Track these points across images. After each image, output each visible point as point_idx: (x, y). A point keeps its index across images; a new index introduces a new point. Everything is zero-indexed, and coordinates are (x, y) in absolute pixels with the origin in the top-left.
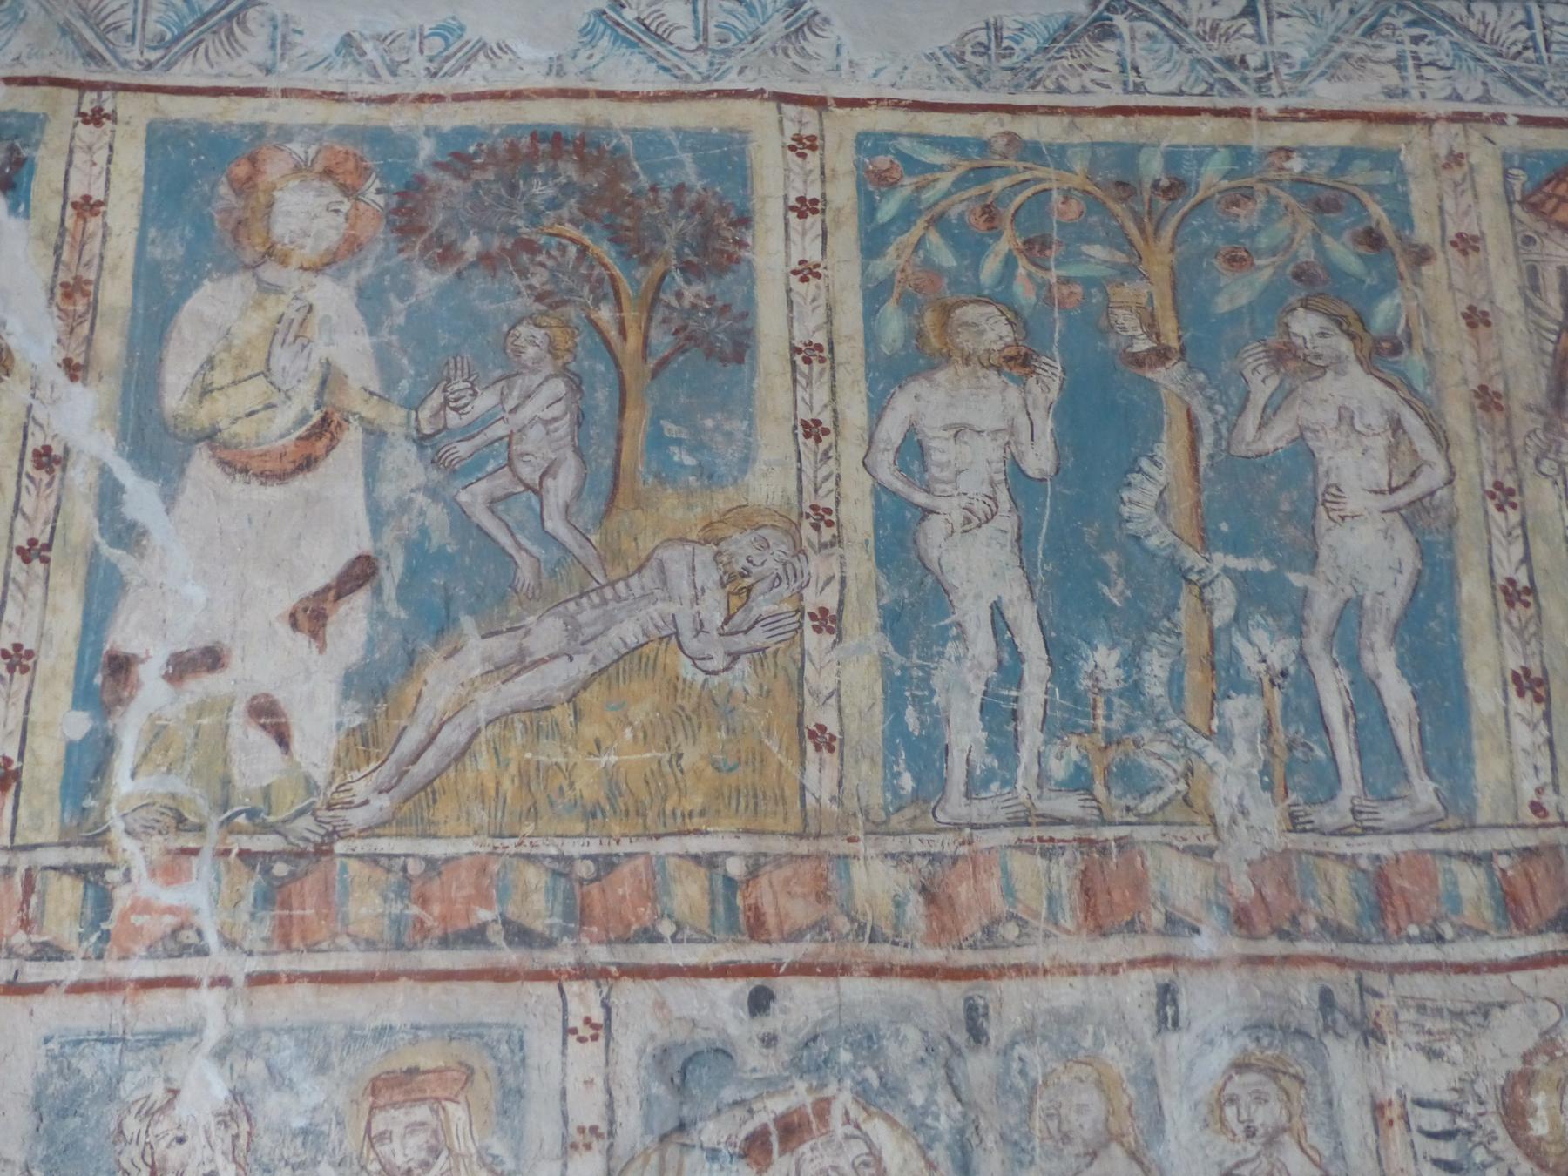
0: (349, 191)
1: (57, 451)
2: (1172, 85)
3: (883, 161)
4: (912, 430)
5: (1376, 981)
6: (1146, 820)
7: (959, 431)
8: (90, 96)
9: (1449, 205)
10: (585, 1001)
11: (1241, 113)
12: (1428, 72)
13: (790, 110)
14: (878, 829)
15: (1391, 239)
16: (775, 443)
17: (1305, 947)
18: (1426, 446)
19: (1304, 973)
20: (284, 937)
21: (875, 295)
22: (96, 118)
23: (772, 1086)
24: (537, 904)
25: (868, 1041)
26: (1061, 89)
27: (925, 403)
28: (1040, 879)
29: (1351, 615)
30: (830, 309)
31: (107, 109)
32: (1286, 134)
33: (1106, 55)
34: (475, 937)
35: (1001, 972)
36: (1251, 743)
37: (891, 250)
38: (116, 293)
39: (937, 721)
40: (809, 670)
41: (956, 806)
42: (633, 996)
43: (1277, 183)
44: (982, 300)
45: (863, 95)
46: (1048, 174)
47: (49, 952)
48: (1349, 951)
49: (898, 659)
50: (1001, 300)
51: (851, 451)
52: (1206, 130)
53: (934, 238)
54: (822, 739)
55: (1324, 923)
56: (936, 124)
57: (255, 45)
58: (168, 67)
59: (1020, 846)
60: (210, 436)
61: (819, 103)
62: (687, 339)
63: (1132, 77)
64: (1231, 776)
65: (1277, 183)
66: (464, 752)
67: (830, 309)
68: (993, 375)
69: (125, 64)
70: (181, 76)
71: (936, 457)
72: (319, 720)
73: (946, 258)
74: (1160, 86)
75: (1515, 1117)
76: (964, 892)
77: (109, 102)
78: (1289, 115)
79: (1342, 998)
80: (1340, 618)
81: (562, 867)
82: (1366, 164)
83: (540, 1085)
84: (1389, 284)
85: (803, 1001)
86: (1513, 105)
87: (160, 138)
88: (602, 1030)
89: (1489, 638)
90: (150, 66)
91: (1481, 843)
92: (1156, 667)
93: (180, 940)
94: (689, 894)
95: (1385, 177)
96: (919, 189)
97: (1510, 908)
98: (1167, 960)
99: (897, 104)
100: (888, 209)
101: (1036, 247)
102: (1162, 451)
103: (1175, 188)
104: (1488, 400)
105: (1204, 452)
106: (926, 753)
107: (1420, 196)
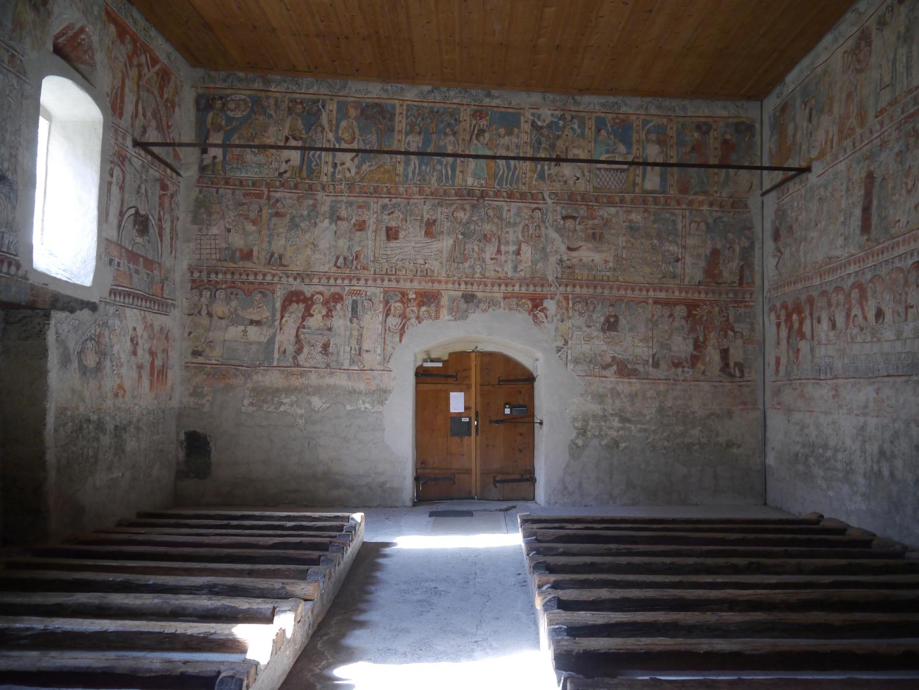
10: (375, 200)
16: (396, 142)
24: (372, 189)
27: (410, 138)
28: (416, 189)
29: (447, 164)
38: (334, 122)
52: (442, 105)
57: (347, 91)
64: (434, 180)
70: (340, 94)
72: (353, 171)
74: (438, 99)
75: (453, 214)
85: (394, 201)
86: (473, 103)
87: (338, 103)
93: (342, 192)
94: (385, 190)
97: (456, 194)
101: (423, 119)
103: (437, 112)
104: (464, 140)
106: (406, 176)
107: (462, 114)
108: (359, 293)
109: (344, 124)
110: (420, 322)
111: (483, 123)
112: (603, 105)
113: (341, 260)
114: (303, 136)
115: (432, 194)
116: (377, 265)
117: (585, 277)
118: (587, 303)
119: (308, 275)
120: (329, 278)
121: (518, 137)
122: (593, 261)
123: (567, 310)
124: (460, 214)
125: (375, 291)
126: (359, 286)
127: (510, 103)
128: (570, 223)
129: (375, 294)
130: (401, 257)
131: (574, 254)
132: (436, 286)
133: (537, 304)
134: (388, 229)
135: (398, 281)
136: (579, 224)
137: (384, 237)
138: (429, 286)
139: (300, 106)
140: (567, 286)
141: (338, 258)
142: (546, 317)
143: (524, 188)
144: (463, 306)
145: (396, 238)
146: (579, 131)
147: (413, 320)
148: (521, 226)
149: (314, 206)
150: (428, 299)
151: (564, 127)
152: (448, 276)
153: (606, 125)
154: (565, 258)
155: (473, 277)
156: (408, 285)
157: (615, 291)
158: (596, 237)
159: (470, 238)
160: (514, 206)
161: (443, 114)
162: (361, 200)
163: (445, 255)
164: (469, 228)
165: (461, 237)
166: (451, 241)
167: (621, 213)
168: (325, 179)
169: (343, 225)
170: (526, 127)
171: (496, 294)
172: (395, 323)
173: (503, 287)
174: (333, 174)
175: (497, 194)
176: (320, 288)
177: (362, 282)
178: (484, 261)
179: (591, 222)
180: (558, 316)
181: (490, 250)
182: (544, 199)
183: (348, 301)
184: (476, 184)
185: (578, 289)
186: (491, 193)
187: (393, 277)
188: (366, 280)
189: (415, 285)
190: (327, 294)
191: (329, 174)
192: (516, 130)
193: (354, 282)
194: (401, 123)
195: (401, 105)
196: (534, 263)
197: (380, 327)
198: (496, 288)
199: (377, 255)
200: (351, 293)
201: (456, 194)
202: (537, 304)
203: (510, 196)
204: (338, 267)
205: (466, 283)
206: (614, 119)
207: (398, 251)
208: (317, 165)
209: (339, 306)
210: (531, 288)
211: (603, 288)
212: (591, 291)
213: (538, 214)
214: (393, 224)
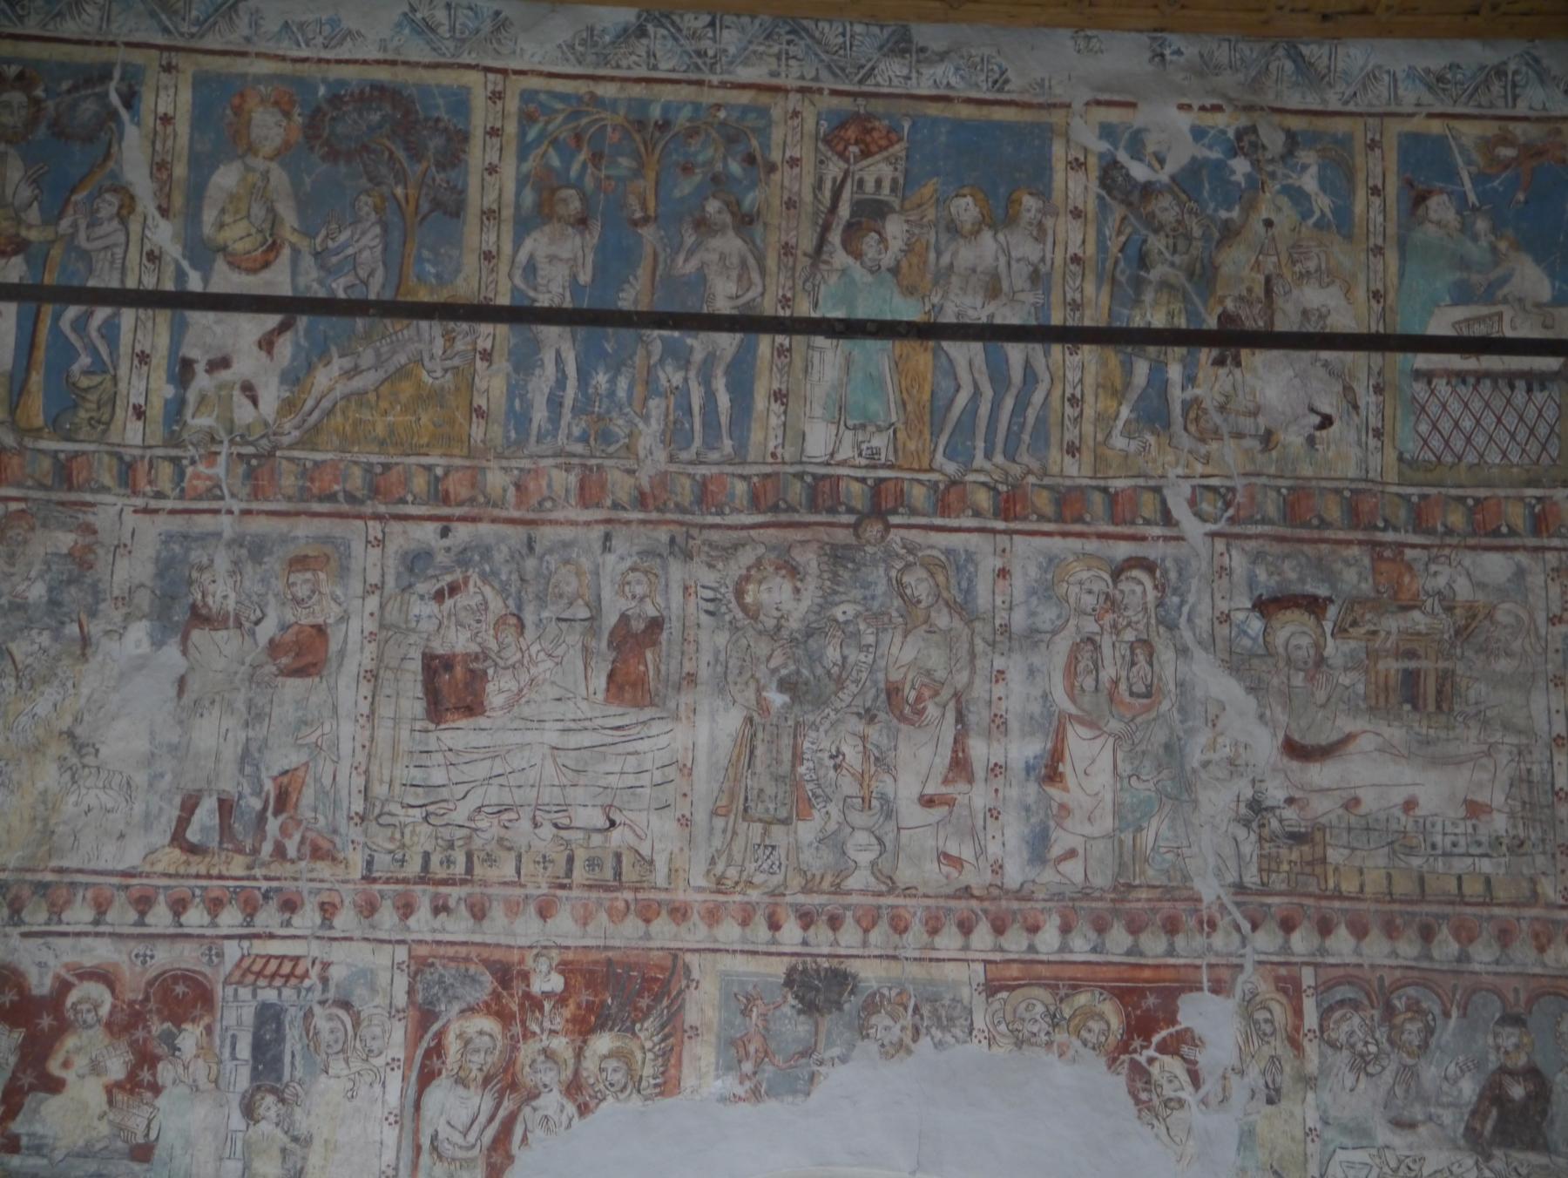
0: (287, 114)
1: (157, 253)
2: (669, 66)
3: (532, 107)
4: (531, 257)
5: (694, 532)
6: (610, 456)
7: (552, 259)
8: (165, 55)
9: (789, 140)
10: (375, 528)
11: (700, 83)
12: (792, 62)
13: (491, 76)
14: (500, 456)
15: (759, 158)
16: (471, 262)
17: (669, 516)
18: (755, 276)
19: (664, 528)
20: (255, 494)
21: (522, 182)
22: (168, 68)
23: (448, 570)
24: (357, 479)
25: (486, 553)
26: (618, 66)
27: (537, 244)
30: (501, 190)
31: (174, 62)
32: (720, 95)
33: (641, 47)
34: (332, 497)
35: (544, 522)
36: (658, 421)
37: (531, 158)
38: (180, 171)
39: (528, 406)
40: (477, 379)
41: (532, 447)
42: (396, 527)
43: (711, 125)
44: (569, 186)
45: (525, 67)
46: (606, 115)
47: (159, 495)
48: (688, 518)
49: (514, 376)
50: (578, 185)
51: (504, 268)
52: (686, 92)
53: (551, 151)
54: (481, 413)
55: (677, 505)
56: (559, 86)
57: (243, 26)
58: (202, 37)
59: (556, 466)
60: (223, 249)
61: (504, 72)
62: (437, 204)
63: (652, 60)
64: (649, 435)
65: (711, 125)
66: (330, 412)
67: (501, 190)
68: (570, 230)
69: (182, 35)
70: (211, 42)
71: (540, 273)
73: (556, 162)
74: (665, 66)
75: (740, 593)
76: (532, 486)
77: (176, 59)
78: (723, 85)
79: (680, 539)
80: (705, 361)
81: (368, 468)
82: (754, 115)
83: (356, 565)
84: (754, 185)
85: (462, 532)
86: (829, 83)
88: (381, 543)
89: (767, 373)
90: (192, 36)
91: (747, 470)
92: (623, 383)
94: (420, 483)
95: (762, 123)
96: (547, 123)
97: (755, 502)
98: (608, 521)
99: (540, 74)
100: (532, 134)
101: (597, 157)
102: (640, 272)
103: (664, 126)
104: (787, 249)
105: (658, 273)
106: (521, 420)
107: (777, 134)
108: (288, 972)
109: (226, 178)
110: (583, 1110)
111: (878, 172)
112: (1437, 82)
113: (206, 814)
114: (33, 235)
115: (641, 501)
116: (382, 839)
117: (1375, 881)
118: (1389, 1011)
119: (42, 888)
120: (143, 903)
121: (1040, 234)
122: (1409, 805)
123: (1296, 1045)
124: (775, 594)
125: (369, 962)
126: (299, 937)
127: (1000, 83)
128: (1292, 630)
129: (367, 976)
130: (494, 795)
131: (1319, 774)
132: (663, 933)
133: (1145, 1015)
134: (435, 667)
135: (479, 913)
136: (1340, 631)
137: (413, 703)
138: (627, 934)
139: (17, 97)
140: (1288, 926)
141: (189, 806)
142: (1195, 1079)
143: (1071, 466)
144: (793, 1027)
145: (473, 707)
146: (1323, 203)
147: (551, 1101)
148: (1063, 645)
149: (81, 560)
150: (624, 993)
151: (1255, 185)
152: (720, 885)
153: (1451, 174)
154: (1276, 793)
155: (837, 890)
156: (529, 929)
157: (1524, 954)
158: (1420, 693)
159: (821, 702)
160: (1027, 553)
161: (692, 132)
162: (304, 529)
163: (704, 785)
164: (814, 659)
165: (777, 699)
166: (732, 721)
167: (1536, 580)
168: (133, 433)
169: (219, 650)
170: (1079, 188)
171: (951, 971)
172: (462, 1116)
173: (982, 936)
174: (176, 409)
175: (947, 498)
176: (102, 952)
177: (307, 919)
178: (889, 812)
179: (1392, 623)
180: (1254, 1074)
181: (918, 760)
182: (1167, 518)
183: (237, 1012)
184: (846, 452)
185: (1342, 943)
186: (918, 494)
187: (455, 893)
188: (328, 910)
189: (564, 927)
190: (134, 981)
191: (156, 410)
192: (1030, 203)
193: (268, 918)
194: (494, 175)
195: (496, 96)
196: (1129, 818)
197: (391, 1135)
198: (949, 941)
199: (380, 790)
200: (249, 973)
201: (755, 502)
202: (1145, 1015)
203: (1009, 505)
204: (192, 849)
205: (807, 919)
206: (1487, 145)
207: (481, 770)
208: (98, 367)
209: (190, 1037)
210: (1119, 939)
211: (1466, 934)
212: (1408, 949)
213: (1139, 589)
214: (459, 642)
